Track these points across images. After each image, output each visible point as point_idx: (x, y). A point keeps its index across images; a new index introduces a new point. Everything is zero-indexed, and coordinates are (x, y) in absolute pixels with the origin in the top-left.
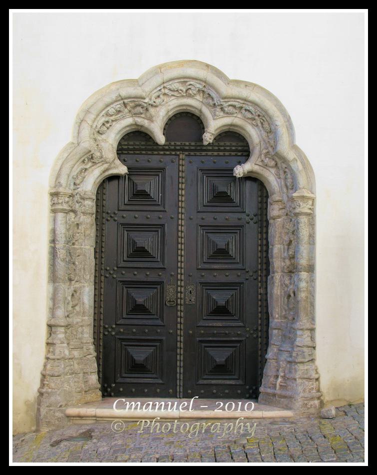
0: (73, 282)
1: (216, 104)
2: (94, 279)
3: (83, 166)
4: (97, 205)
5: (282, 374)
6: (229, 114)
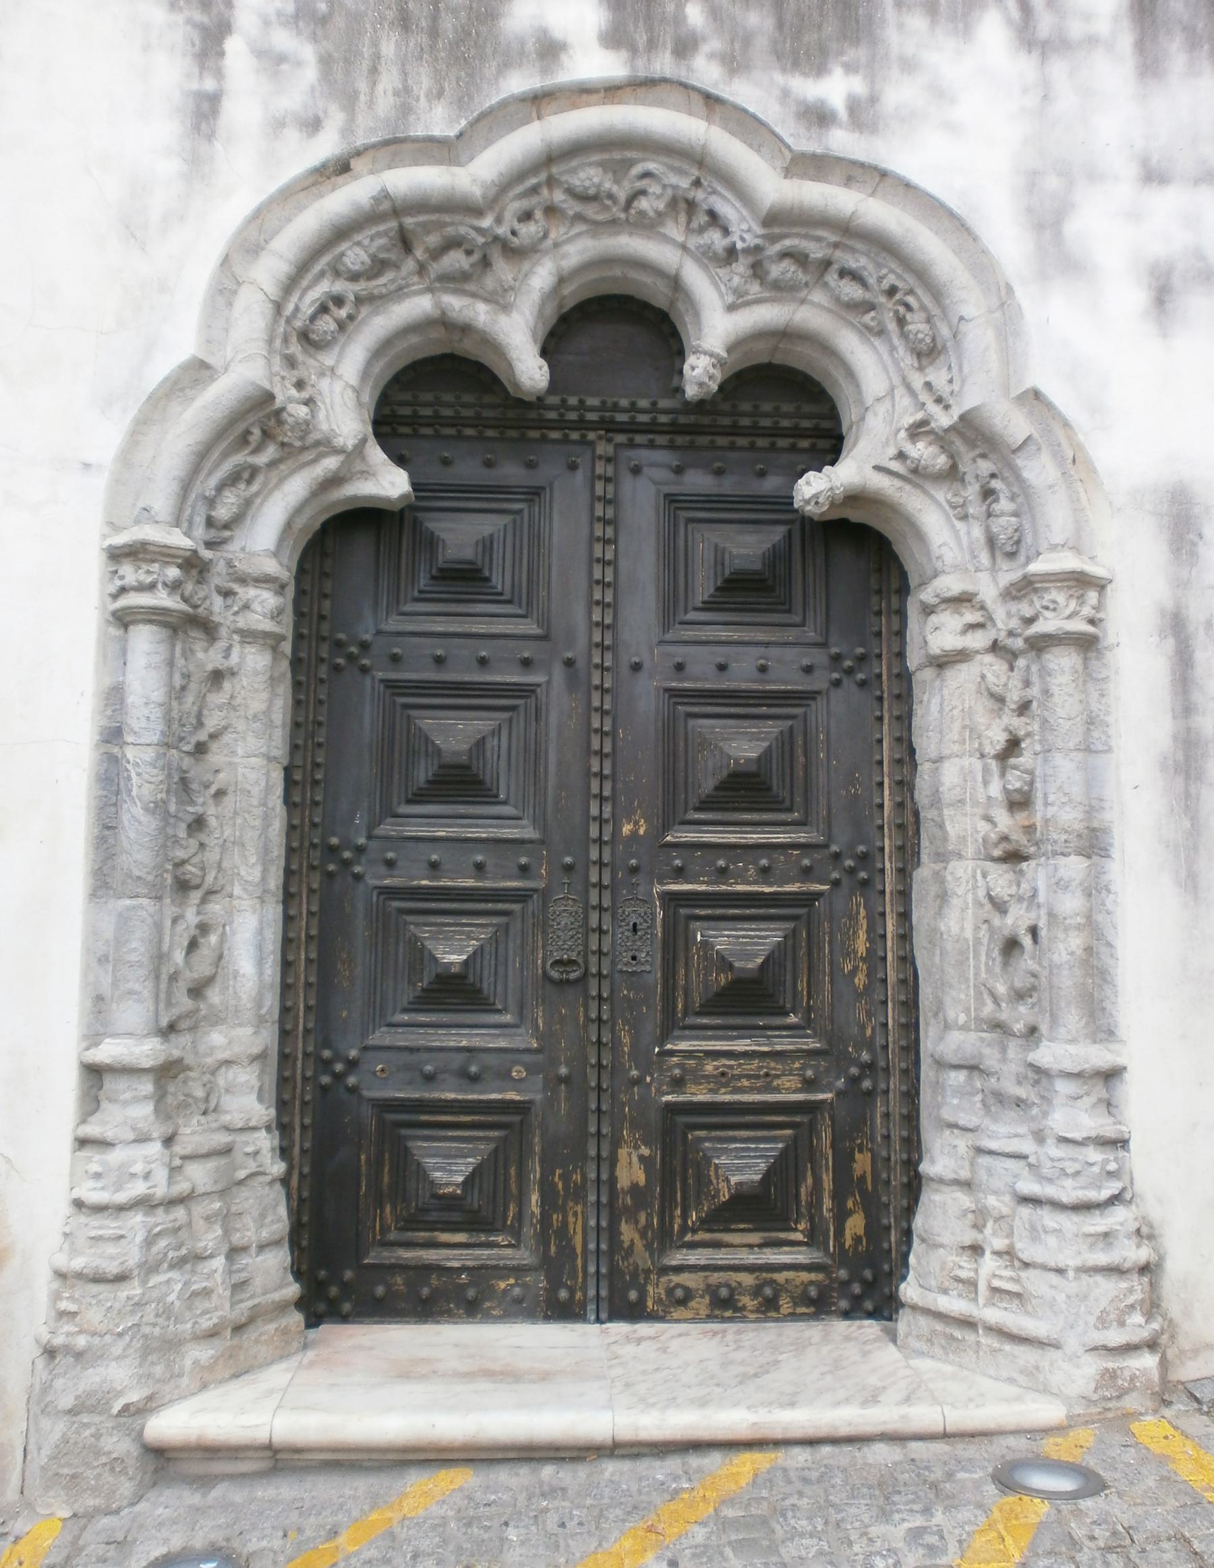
0: (195, 896)
1: (739, 245)
2: (281, 881)
3: (239, 458)
4: (299, 614)
5: (1000, 1243)
6: (781, 290)
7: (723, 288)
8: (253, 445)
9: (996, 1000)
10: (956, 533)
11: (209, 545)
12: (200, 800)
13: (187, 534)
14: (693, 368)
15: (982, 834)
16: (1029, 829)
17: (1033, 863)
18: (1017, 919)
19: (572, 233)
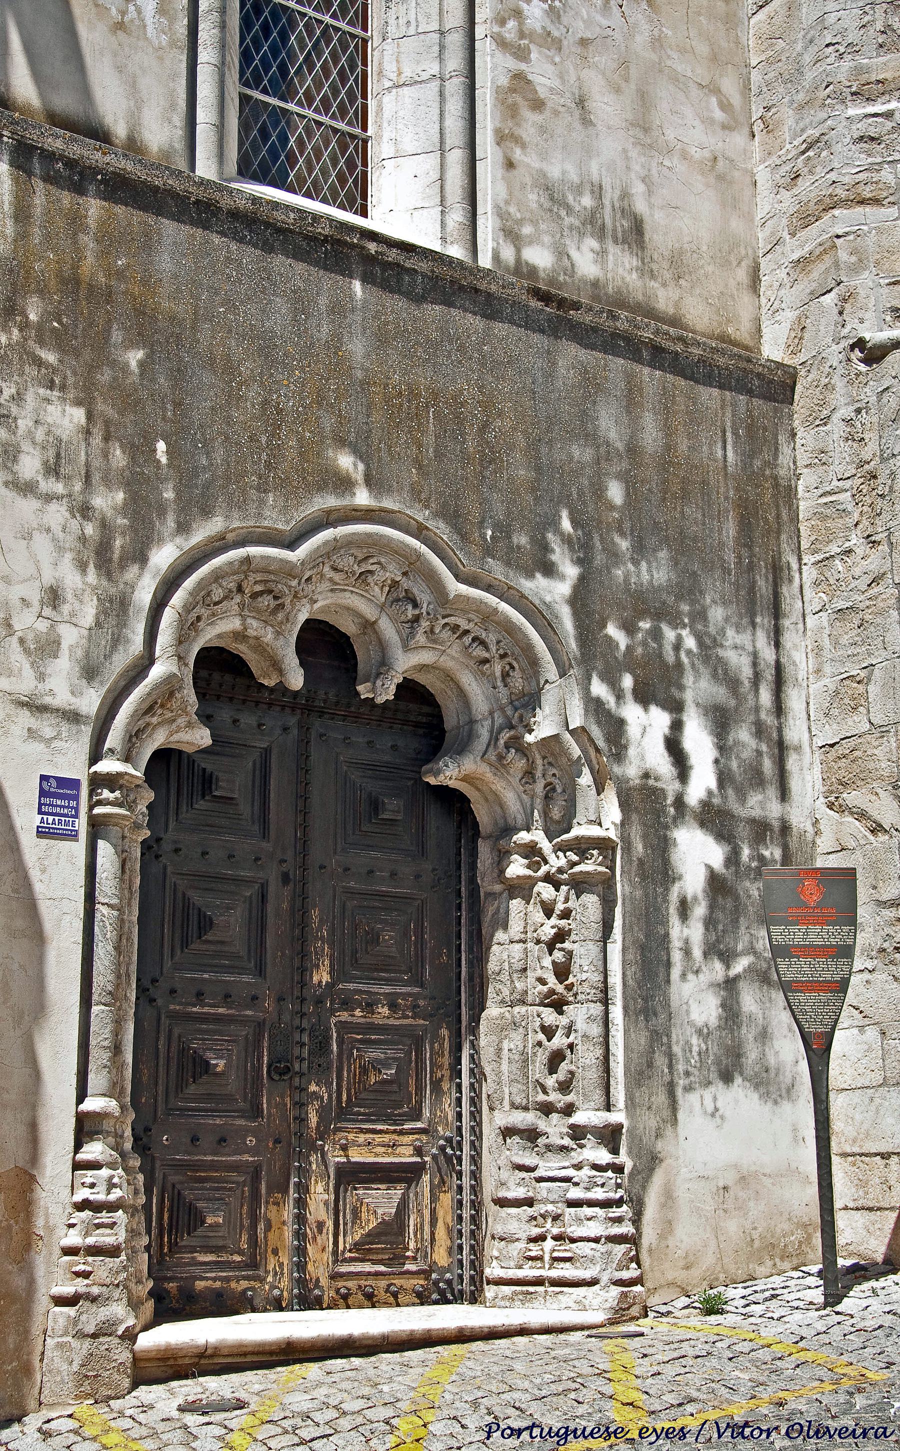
18: (559, 1041)
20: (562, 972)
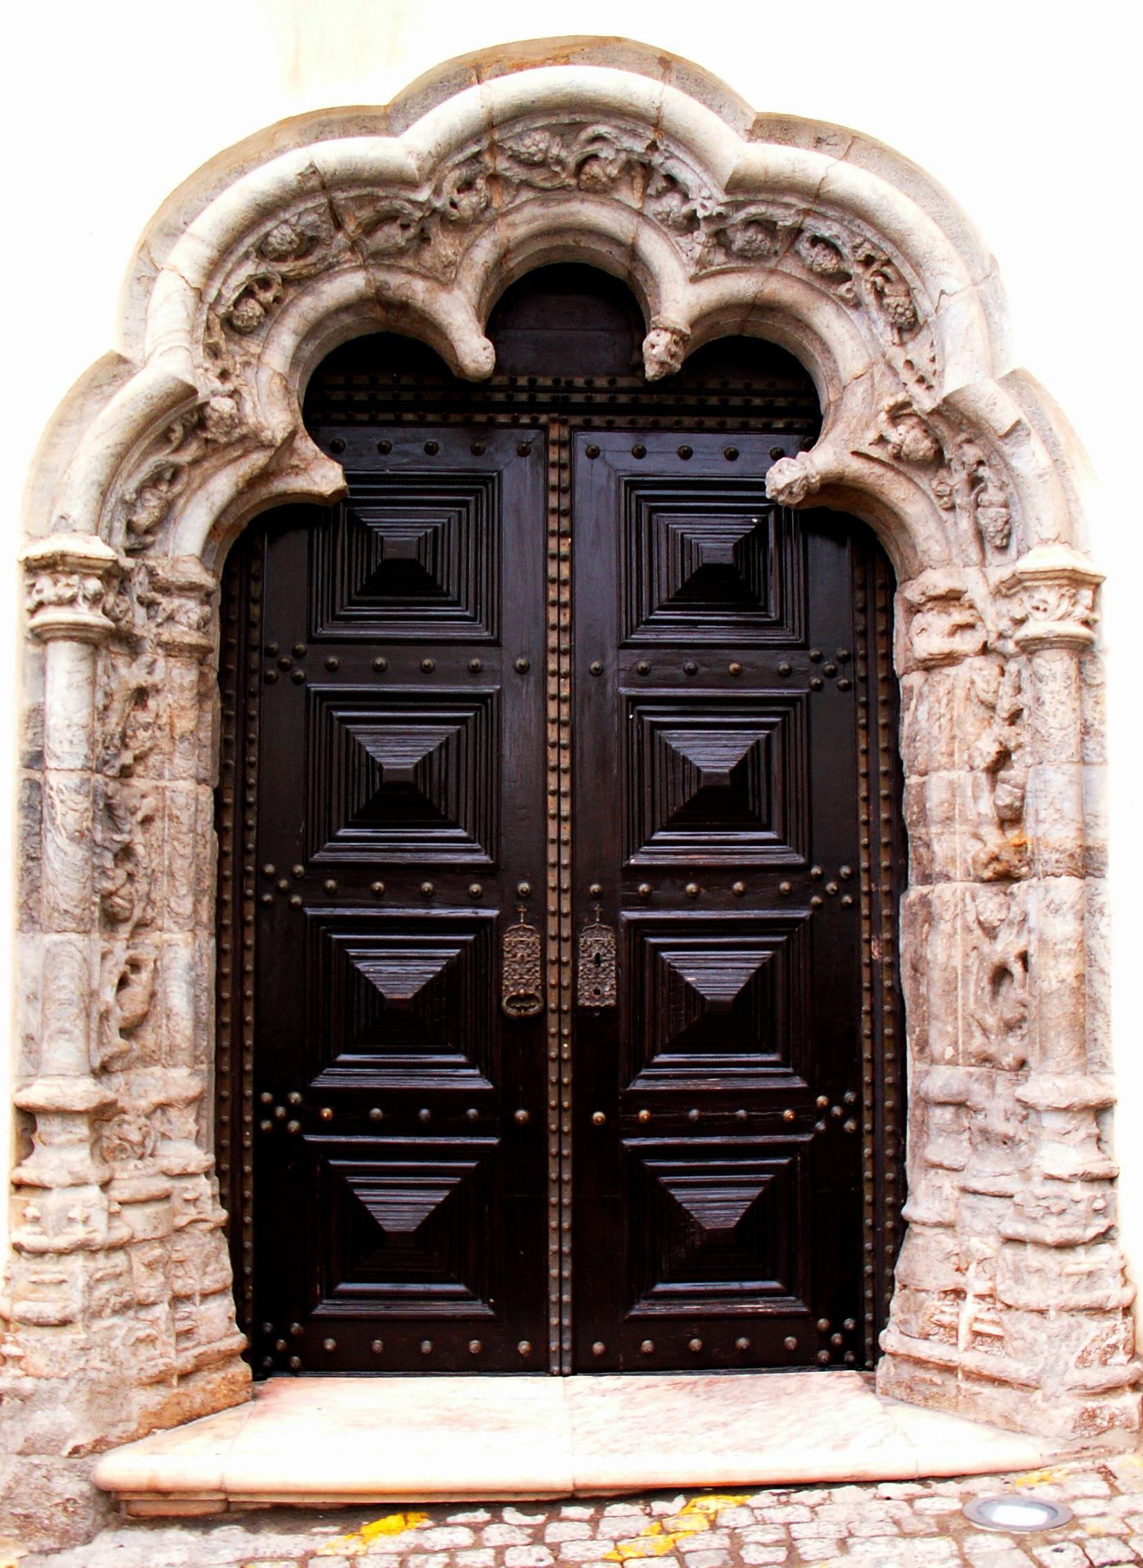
0: (124, 931)
1: (701, 213)
3: (163, 456)
4: (226, 625)
5: (982, 1287)
6: (749, 258)
7: (684, 257)
8: (175, 443)
9: (985, 1031)
10: (941, 522)
11: (130, 552)
12: (127, 828)
13: (108, 542)
14: (653, 346)
15: (972, 853)
16: (1020, 848)
17: (1024, 884)
18: (1006, 947)
19: (518, 202)
20: (1011, 818)
